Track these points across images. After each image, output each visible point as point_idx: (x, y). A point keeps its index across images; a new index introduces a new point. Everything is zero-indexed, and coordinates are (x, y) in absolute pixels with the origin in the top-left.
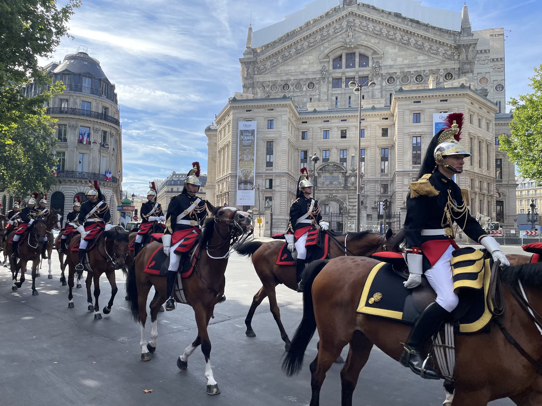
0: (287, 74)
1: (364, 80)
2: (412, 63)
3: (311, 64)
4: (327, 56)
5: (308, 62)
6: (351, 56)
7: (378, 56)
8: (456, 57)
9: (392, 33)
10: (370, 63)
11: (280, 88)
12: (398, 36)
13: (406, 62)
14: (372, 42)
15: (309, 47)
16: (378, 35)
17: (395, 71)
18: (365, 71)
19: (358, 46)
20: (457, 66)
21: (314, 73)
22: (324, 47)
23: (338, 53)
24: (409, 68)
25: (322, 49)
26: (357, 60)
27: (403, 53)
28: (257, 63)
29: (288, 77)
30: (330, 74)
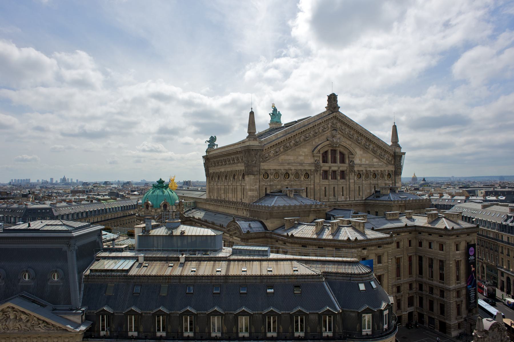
0: (289, 164)
1: (343, 175)
2: (370, 163)
3: (306, 156)
4: (319, 151)
5: (304, 154)
6: (334, 152)
7: (353, 156)
8: (393, 162)
9: (360, 138)
10: (347, 161)
11: (282, 177)
12: (363, 141)
13: (367, 162)
14: (347, 143)
15: (305, 140)
16: (350, 138)
17: (362, 169)
18: (344, 167)
19: (340, 146)
20: (393, 170)
21: (310, 164)
22: (315, 142)
23: (326, 149)
24: (369, 167)
25: (314, 143)
26: (338, 157)
27: (365, 155)
28: (263, 150)
29: (289, 167)
30: (321, 167)
